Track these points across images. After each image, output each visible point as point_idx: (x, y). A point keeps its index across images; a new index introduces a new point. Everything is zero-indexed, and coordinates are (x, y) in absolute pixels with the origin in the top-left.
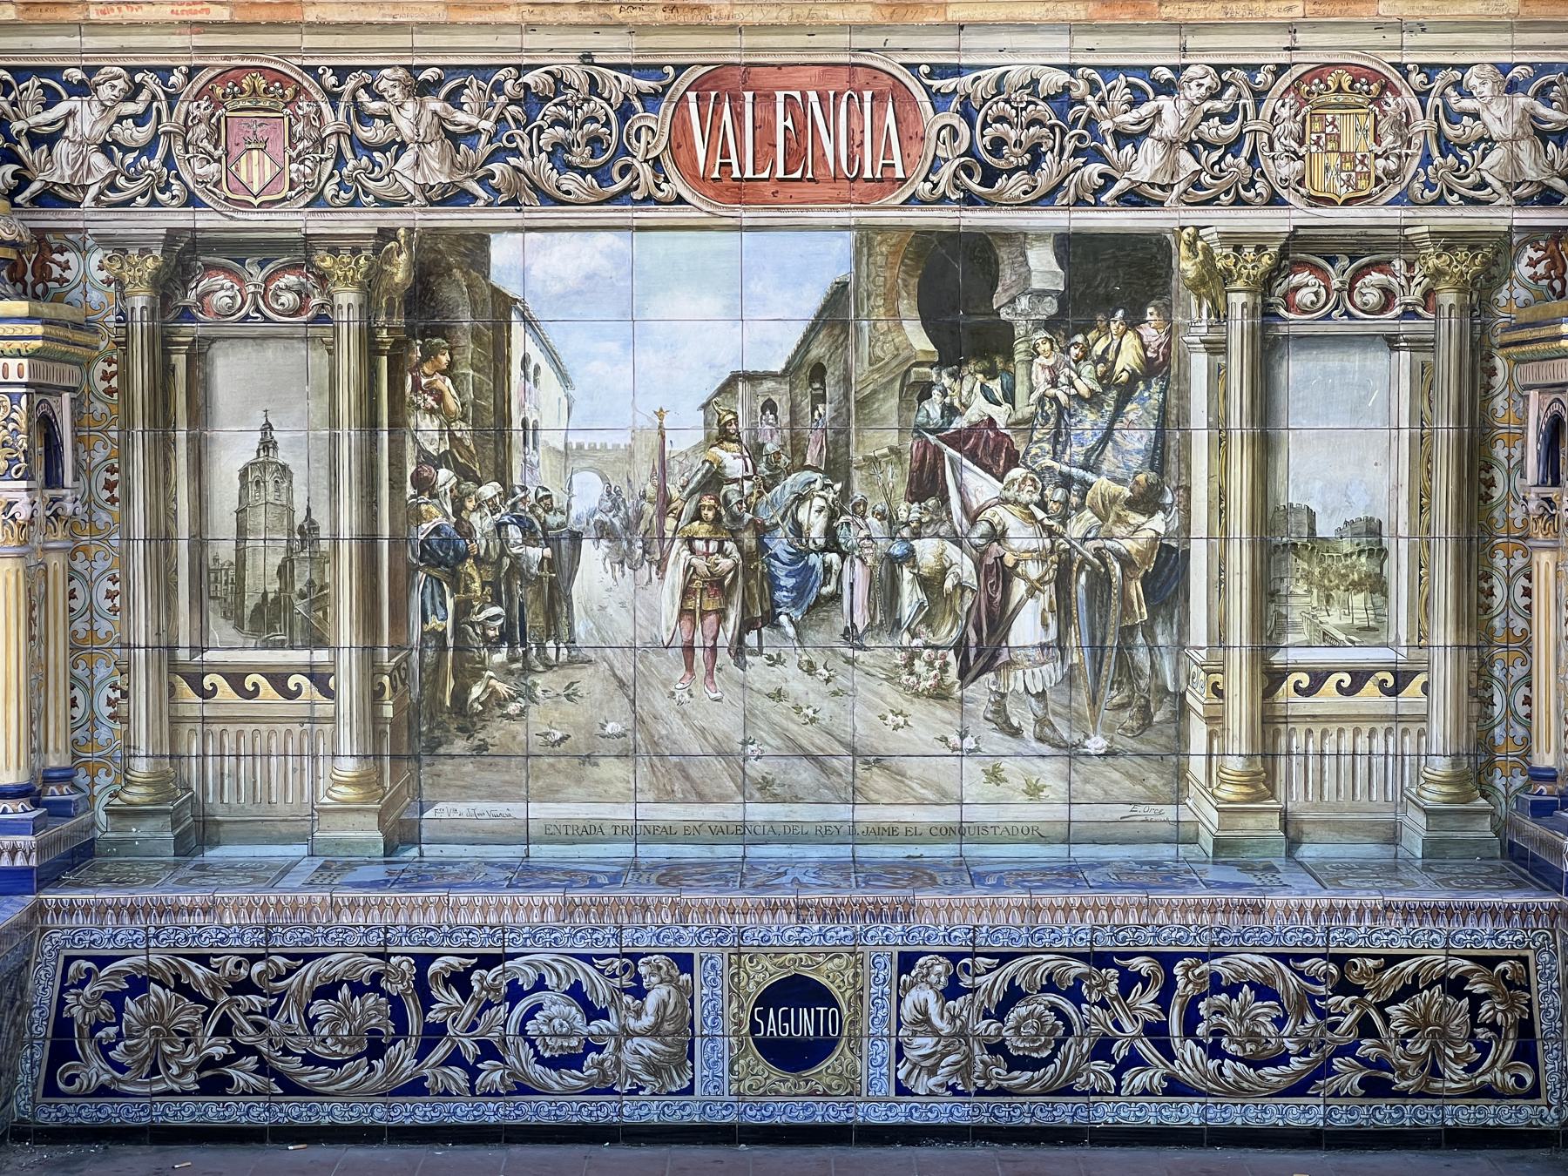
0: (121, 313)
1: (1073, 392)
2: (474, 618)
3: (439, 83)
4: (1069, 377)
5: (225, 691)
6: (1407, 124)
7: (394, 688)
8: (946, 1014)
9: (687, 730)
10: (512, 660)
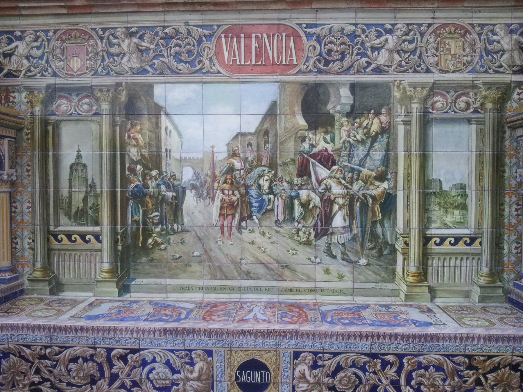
0: (32, 113)
1: (355, 139)
2: (149, 216)
3: (137, 33)
4: (354, 134)
5: (65, 240)
6: (474, 45)
7: (122, 240)
8: (312, 375)
9: (221, 255)
10: (162, 230)
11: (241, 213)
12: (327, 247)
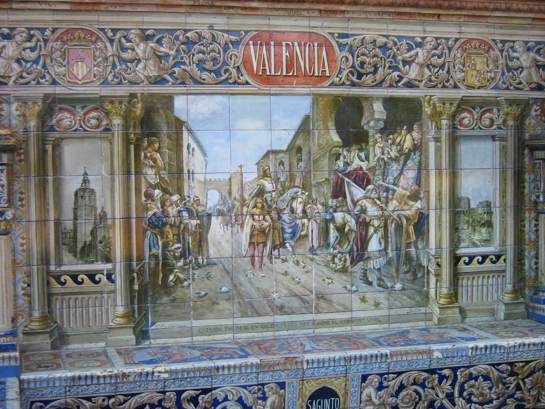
0: (25, 129)
1: (389, 156)
2: (170, 249)
3: (153, 36)
4: (388, 151)
5: (70, 282)
6: (497, 61)
7: (138, 278)
8: (378, 397)
9: (252, 289)
10: (185, 264)
11: (273, 241)
12: (364, 273)
